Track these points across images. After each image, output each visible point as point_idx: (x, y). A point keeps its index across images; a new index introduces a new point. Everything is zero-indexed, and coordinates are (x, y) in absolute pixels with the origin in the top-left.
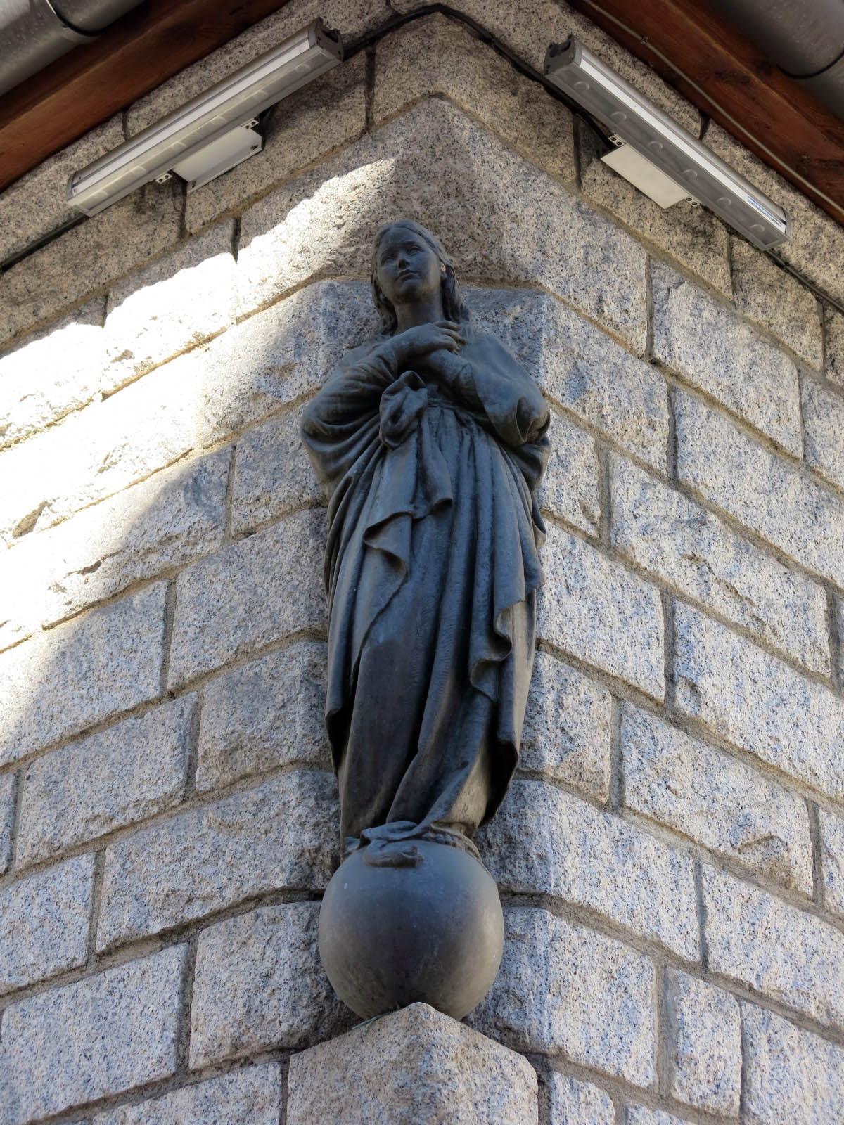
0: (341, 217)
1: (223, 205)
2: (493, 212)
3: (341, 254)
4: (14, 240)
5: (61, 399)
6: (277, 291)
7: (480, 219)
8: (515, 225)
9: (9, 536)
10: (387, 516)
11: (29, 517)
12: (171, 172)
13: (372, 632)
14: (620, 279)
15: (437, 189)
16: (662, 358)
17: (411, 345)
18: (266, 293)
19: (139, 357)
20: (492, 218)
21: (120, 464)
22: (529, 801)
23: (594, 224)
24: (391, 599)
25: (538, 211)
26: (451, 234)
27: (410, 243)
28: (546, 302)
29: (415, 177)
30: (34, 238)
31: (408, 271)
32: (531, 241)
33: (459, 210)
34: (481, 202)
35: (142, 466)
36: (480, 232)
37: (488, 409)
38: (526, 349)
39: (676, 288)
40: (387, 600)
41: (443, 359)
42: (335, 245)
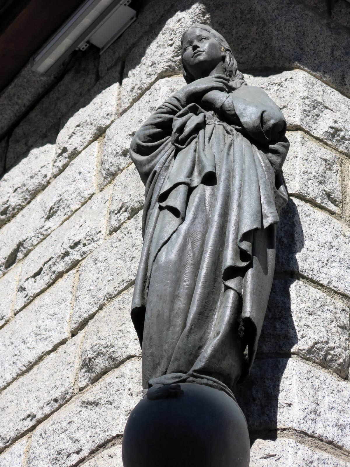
0: (172, 40)
1: (117, 55)
3: (173, 61)
4: (17, 107)
5: (32, 184)
6: (140, 91)
8: (280, 32)
9: (3, 268)
10: (171, 186)
11: (12, 254)
12: (88, 42)
13: (158, 255)
18: (134, 94)
19: (70, 149)
20: (265, 29)
21: (59, 212)
23: (339, 34)
24: (172, 235)
25: (297, 24)
30: (27, 104)
32: (292, 42)
34: (257, 19)
35: (68, 210)
37: (243, 120)
42: (169, 57)
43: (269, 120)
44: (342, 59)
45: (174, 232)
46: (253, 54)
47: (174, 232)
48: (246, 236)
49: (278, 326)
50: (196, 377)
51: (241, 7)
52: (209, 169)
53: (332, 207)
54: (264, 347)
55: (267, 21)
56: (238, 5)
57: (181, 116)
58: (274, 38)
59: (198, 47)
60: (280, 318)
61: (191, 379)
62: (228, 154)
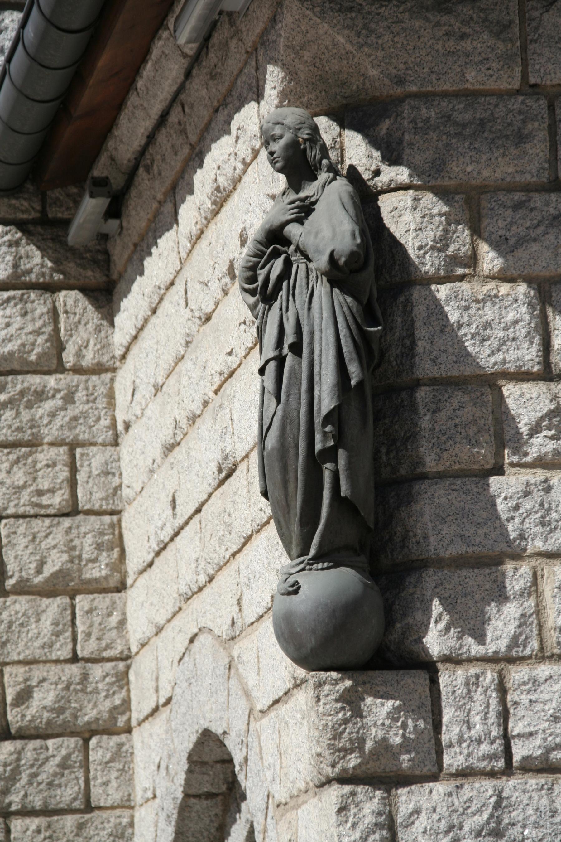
16: (539, 81)
17: (271, 226)
20: (355, 60)
25: (391, 35)
27: (273, 135)
29: (298, 48)
39: (547, 11)
41: (290, 232)
43: (339, 259)
46: (355, 87)
48: (327, 419)
49: (409, 447)
51: (324, 43)
53: (460, 271)
54: (401, 469)
55: (354, 52)
56: (320, 42)
57: (262, 268)
58: (369, 67)
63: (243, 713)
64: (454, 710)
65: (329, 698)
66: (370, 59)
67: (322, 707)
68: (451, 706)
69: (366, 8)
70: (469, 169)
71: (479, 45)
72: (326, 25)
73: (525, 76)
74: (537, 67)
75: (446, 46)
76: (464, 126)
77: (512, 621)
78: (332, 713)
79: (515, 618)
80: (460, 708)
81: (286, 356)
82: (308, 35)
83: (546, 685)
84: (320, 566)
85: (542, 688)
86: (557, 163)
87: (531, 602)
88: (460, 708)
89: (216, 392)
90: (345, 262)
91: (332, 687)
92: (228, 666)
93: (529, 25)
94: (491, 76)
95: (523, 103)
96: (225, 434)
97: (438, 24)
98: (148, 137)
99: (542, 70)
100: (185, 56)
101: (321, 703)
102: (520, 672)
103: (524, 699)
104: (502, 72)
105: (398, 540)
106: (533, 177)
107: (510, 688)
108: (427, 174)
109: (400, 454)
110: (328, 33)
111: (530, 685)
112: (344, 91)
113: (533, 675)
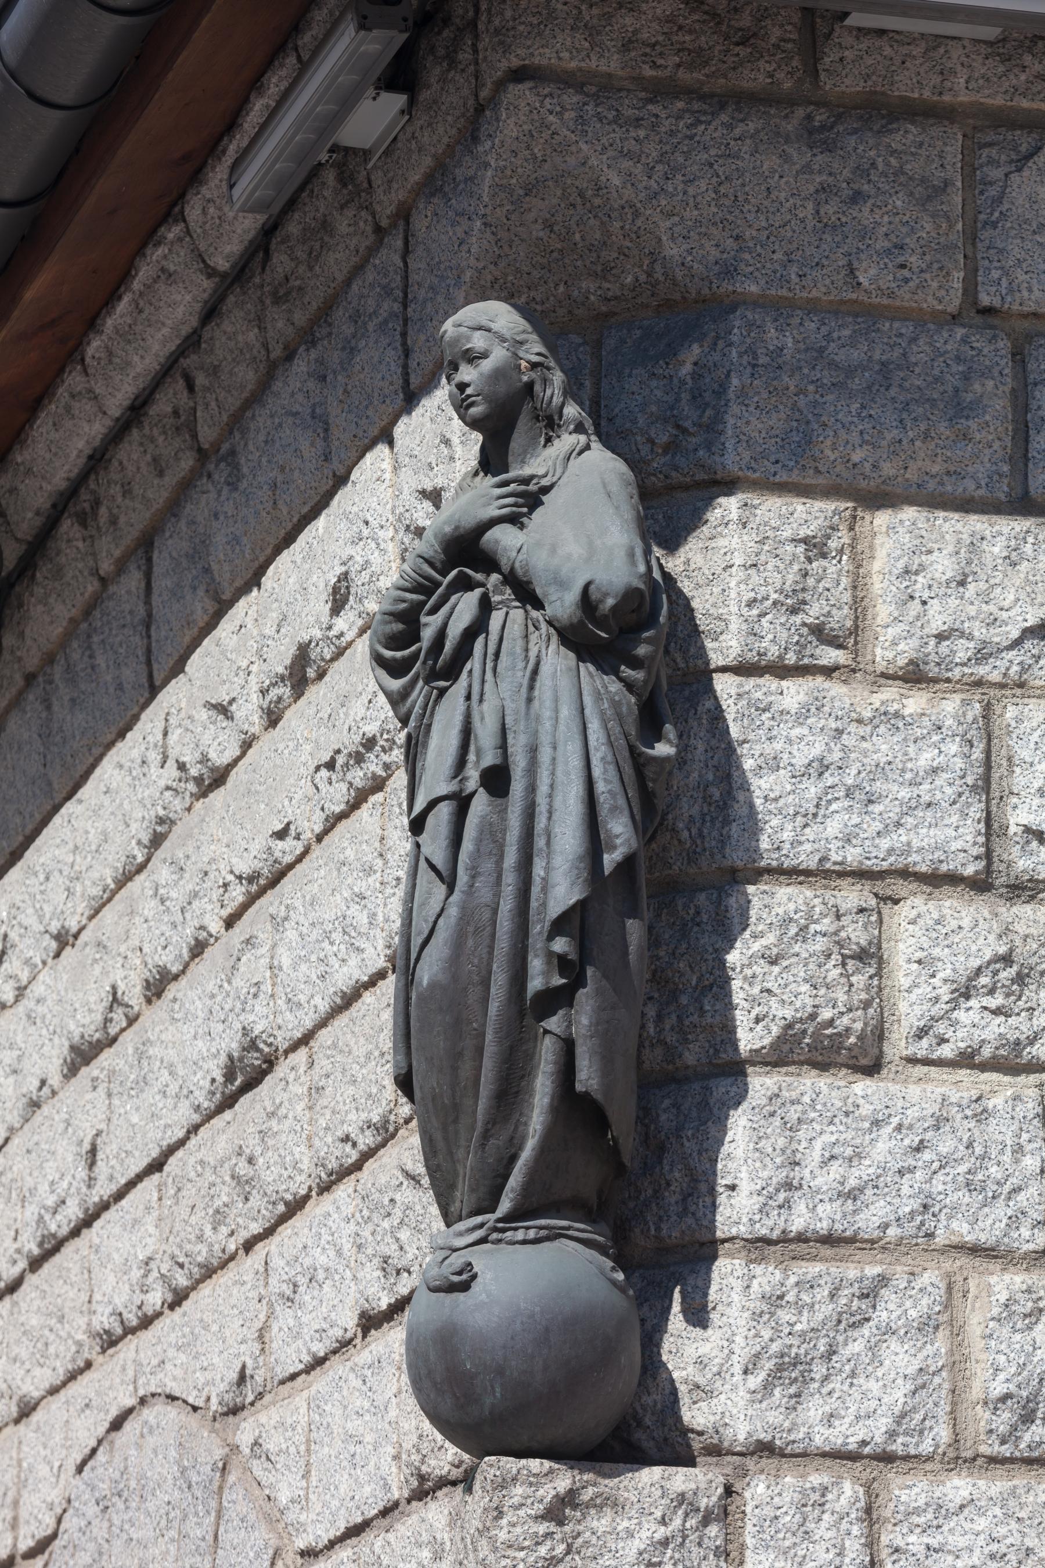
2: (637, 214)
7: (622, 228)
8: (676, 219)
14: (886, 219)
15: (555, 201)
16: (997, 302)
17: (457, 528)
20: (639, 223)
22: (715, 1111)
24: (435, 922)
25: (715, 179)
26: (594, 255)
27: (468, 350)
28: (737, 323)
29: (521, 192)
31: (469, 396)
33: (592, 221)
36: (629, 244)
38: (709, 412)
39: (1019, 170)
40: (430, 925)
41: (497, 542)
43: (601, 601)
44: (844, 220)
45: (439, 916)
46: (629, 279)
47: (439, 916)
48: (559, 926)
49: (707, 1008)
50: (503, 1230)
51: (577, 183)
52: (489, 759)
53: (830, 656)
54: (687, 1054)
55: (639, 205)
56: (569, 181)
57: (434, 611)
58: (664, 238)
59: (468, 385)
60: (711, 986)
61: (495, 1236)
62: (529, 700)
63: (257, 1556)
64: (772, 1556)
65: (521, 1513)
66: (668, 224)
67: (505, 1530)
68: (768, 1547)
69: (667, 123)
70: (856, 457)
71: (886, 219)
72: (584, 147)
73: (970, 289)
74: (995, 274)
75: (822, 212)
76: (850, 372)
77: (900, 1381)
78: (527, 1543)
79: (905, 1376)
80: (785, 1553)
81: (472, 795)
82: (546, 166)
83: (961, 1517)
84: (520, 1235)
85: (952, 1524)
86: (1026, 465)
87: (941, 1344)
88: (785, 1553)
89: (230, 923)
90: (615, 609)
91: (530, 1491)
92: (220, 1465)
93: (982, 193)
94: (906, 281)
95: (964, 341)
96: (255, 996)
97: (807, 168)
98: (90, 457)
99: (1004, 282)
100: (210, 272)
101: (504, 1522)
102: (909, 1487)
103: (915, 1542)
104: (928, 276)
105: (673, 1200)
106: (979, 487)
107: (886, 1520)
108: (773, 459)
109: (687, 1023)
110: (590, 163)
111: (930, 1516)
112: (607, 285)
113: (937, 1494)
